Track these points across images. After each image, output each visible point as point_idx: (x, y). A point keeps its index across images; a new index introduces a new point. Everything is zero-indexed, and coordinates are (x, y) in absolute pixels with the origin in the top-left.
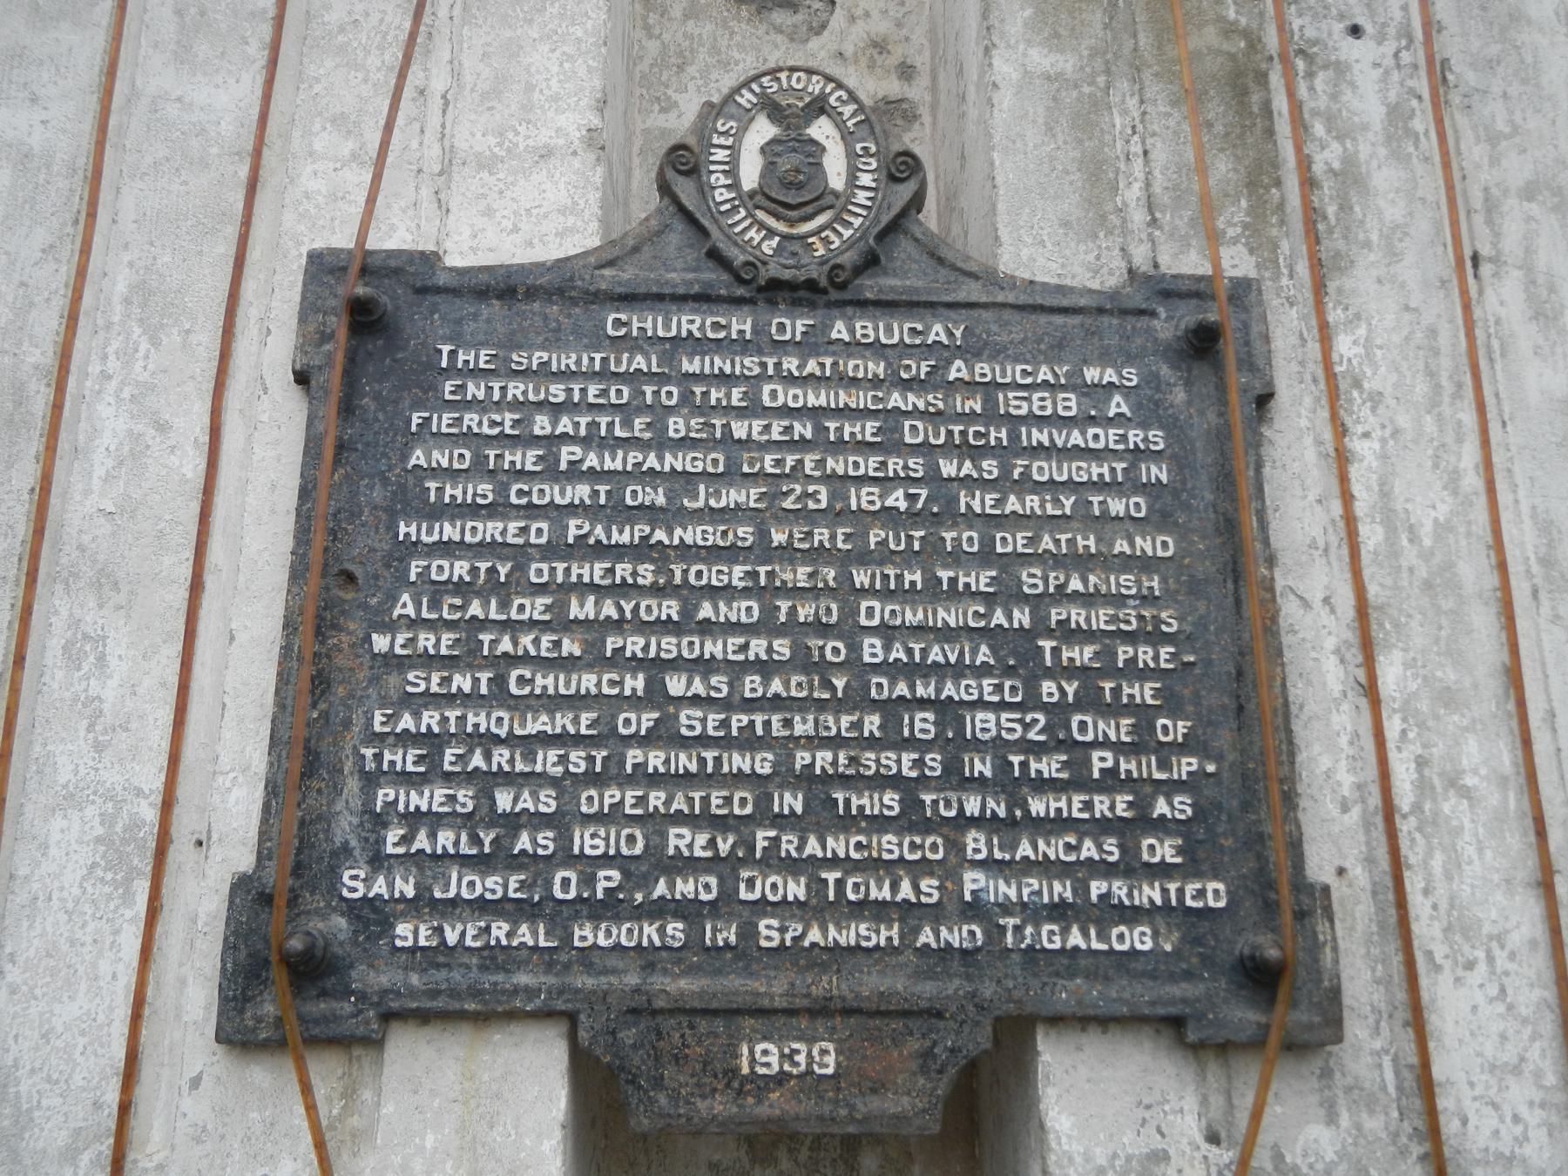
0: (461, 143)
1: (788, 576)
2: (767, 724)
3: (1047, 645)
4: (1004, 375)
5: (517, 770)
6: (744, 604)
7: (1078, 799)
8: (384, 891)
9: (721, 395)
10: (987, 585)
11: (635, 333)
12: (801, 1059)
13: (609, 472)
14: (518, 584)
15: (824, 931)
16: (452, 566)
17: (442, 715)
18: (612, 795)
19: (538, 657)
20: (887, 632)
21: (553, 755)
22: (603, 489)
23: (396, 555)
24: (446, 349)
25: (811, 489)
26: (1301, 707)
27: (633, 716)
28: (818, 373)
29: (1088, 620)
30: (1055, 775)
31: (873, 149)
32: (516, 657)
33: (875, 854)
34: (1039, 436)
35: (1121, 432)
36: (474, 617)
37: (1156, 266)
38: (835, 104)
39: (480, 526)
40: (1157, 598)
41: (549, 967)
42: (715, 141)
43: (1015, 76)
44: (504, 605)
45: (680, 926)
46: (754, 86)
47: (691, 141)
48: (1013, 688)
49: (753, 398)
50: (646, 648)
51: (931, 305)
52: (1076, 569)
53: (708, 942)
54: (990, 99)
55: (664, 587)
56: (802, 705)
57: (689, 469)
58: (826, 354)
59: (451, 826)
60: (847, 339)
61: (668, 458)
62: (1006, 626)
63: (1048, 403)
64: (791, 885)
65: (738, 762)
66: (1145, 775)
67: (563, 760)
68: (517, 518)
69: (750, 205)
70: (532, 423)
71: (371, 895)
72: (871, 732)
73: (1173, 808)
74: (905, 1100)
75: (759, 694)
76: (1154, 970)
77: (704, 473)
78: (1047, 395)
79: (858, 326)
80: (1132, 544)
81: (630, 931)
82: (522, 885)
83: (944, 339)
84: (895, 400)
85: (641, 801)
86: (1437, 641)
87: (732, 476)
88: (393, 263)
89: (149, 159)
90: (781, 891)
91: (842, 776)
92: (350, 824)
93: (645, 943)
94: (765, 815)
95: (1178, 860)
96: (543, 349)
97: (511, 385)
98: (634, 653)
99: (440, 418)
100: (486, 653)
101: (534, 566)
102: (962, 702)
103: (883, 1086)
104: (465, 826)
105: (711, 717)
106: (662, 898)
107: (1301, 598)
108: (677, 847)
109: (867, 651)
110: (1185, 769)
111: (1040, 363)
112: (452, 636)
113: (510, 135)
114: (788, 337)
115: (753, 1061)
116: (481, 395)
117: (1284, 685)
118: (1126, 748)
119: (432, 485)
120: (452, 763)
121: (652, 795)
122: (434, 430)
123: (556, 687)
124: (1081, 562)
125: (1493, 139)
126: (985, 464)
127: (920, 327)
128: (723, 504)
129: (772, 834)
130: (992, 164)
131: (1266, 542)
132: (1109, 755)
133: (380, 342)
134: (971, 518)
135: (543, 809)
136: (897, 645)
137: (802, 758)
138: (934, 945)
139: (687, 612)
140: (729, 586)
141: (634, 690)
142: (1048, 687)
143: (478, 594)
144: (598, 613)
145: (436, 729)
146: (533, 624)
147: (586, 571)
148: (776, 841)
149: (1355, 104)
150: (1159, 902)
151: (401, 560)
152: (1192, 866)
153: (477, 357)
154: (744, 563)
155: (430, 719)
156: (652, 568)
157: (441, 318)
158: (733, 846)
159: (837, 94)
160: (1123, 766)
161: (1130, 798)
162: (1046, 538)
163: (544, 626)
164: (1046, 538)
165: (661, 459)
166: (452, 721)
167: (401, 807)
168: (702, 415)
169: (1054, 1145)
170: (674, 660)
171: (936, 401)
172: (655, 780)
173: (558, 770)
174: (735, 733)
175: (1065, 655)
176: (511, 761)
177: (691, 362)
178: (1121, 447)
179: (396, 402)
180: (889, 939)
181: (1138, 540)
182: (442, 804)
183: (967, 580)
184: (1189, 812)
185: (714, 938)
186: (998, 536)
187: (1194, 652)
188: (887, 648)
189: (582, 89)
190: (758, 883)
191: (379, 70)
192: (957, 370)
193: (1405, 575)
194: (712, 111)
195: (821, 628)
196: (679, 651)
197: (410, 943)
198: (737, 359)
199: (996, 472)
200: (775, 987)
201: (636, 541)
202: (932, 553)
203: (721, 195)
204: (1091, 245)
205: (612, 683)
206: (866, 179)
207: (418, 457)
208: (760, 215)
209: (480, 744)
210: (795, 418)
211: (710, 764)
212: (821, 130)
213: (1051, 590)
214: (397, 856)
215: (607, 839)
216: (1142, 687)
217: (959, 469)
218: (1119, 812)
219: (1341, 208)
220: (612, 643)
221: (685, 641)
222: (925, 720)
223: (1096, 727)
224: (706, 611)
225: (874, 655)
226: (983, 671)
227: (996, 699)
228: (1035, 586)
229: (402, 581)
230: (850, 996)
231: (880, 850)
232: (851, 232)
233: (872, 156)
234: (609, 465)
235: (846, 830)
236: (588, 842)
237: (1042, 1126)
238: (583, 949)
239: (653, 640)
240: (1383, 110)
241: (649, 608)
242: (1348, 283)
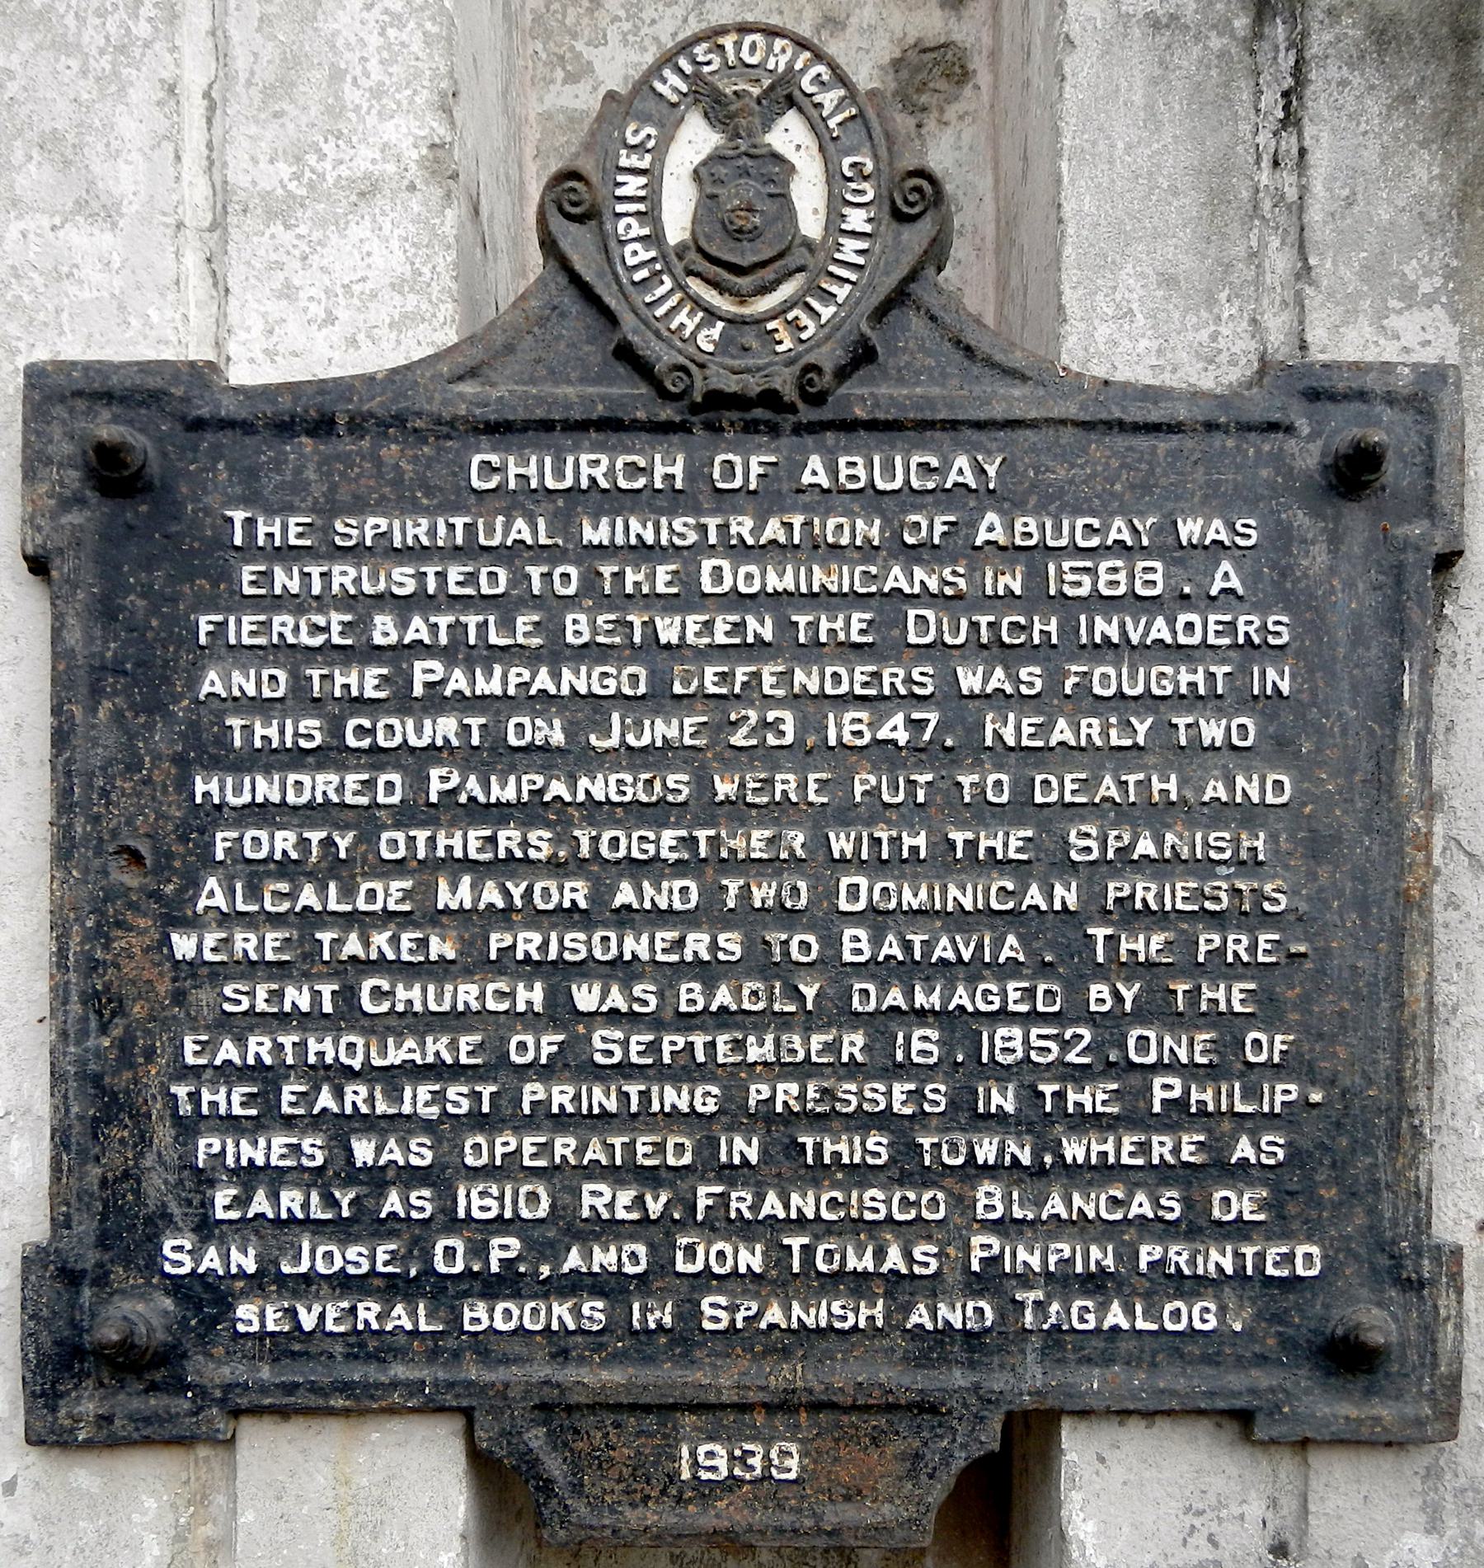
0: (238, 175)
1: (738, 843)
2: (711, 1046)
3: (1100, 932)
5: (378, 1111)
6: (678, 884)
8: (217, 1265)
9: (640, 577)
10: (1019, 850)
11: (512, 485)
12: (756, 1461)
13: (484, 697)
14: (364, 861)
15: (787, 1311)
16: (272, 837)
17: (274, 1041)
18: (505, 1143)
20: (877, 919)
21: (424, 1092)
22: (475, 722)
23: (195, 823)
24: (239, 516)
26: (1454, 1010)
27: (529, 1040)
28: (782, 540)
29: (1160, 896)
30: (1100, 1109)
31: (869, 167)
32: (369, 962)
33: (854, 1213)
34: (1106, 628)
35: (1227, 618)
37: (1303, 346)
38: (809, 89)
39: (306, 779)
40: (1261, 863)
41: (433, 1355)
42: (624, 162)
44: (348, 893)
45: (600, 1305)
46: (683, 63)
47: (587, 166)
49: (687, 579)
50: (544, 947)
51: (953, 425)
52: (1149, 825)
53: (636, 1324)
54: (1059, 66)
55: (566, 862)
56: (758, 1022)
58: (793, 509)
59: (296, 1185)
60: (826, 484)
62: (1044, 907)
63: (1121, 577)
65: (673, 1097)
66: (1224, 1108)
67: (439, 1097)
68: (357, 769)
69: (679, 269)
71: (201, 1270)
72: (852, 1055)
73: (1259, 1150)
74: (886, 1509)
75: (699, 1007)
76: (1218, 1354)
77: (619, 696)
78: (1119, 563)
79: (842, 461)
80: (1231, 786)
81: (535, 1311)
84: (896, 578)
85: (546, 1149)
87: (660, 700)
88: (153, 382)
90: (730, 1262)
92: (166, 1182)
93: (555, 1326)
94: (709, 1166)
95: (1261, 1217)
97: (336, 569)
98: (527, 953)
99: (239, 622)
100: (326, 957)
101: (385, 836)
102: (978, 1013)
103: (859, 1493)
104: (315, 1184)
105: (634, 1039)
108: (592, 1208)
109: (847, 945)
111: (1112, 514)
112: (279, 935)
113: (312, 159)
114: (737, 483)
115: (695, 1464)
116: (294, 586)
118: (1201, 1071)
119: (235, 722)
120: (292, 1104)
121: (559, 1142)
122: (232, 641)
123: (425, 1003)
124: (1155, 814)
126: (1023, 674)
127: (934, 462)
128: (646, 740)
129: (718, 1189)
130: (1059, 181)
131: (1426, 779)
132: (1176, 1082)
133: (143, 508)
134: (1003, 754)
135: (415, 1161)
136: (890, 937)
137: (758, 1092)
138: (929, 1326)
139: (601, 894)
140: (657, 858)
141: (529, 1003)
143: (311, 876)
144: (477, 899)
146: (388, 916)
147: (457, 842)
148: (724, 1198)
150: (1229, 1271)
151: (202, 831)
152: (1280, 1222)
153: (285, 528)
154: (677, 825)
155: (259, 1047)
156: (547, 835)
157: (231, 468)
159: (813, 72)
160: (1195, 1096)
161: (1202, 1138)
162: (1108, 780)
163: (403, 920)
164: (1108, 780)
165: (556, 676)
166: (289, 1049)
167: (230, 1161)
169: (1075, 1555)
170: (583, 962)
172: (562, 1121)
173: (433, 1111)
174: (667, 1060)
175: (1124, 946)
177: (596, 527)
179: (174, 600)
180: (871, 1318)
181: (1240, 781)
182: (282, 1157)
183: (991, 843)
186: (1039, 778)
187: (1308, 939)
188: (877, 942)
189: (418, 75)
190: (700, 1250)
191: (102, 52)
192: (990, 528)
194: (619, 107)
195: (786, 916)
196: (590, 950)
197: (255, 1328)
198: (664, 521)
199: (1039, 683)
200: (724, 1378)
201: (525, 797)
202: (947, 804)
204: (1204, 314)
205: (500, 995)
206: (856, 219)
207: (212, 682)
208: (695, 286)
209: (328, 1079)
210: (747, 611)
211: (634, 1100)
212: (788, 135)
213: (1110, 855)
214: (230, 1222)
216: (1229, 989)
217: (985, 681)
218: (1185, 1157)
220: (497, 941)
222: (925, 1039)
223: (1160, 1044)
224: (625, 895)
225: (859, 952)
226: (1012, 969)
227: (1024, 1008)
228: (1088, 850)
229: (208, 861)
230: (818, 1388)
231: (861, 1208)
232: (833, 309)
233: (866, 178)
234: (482, 687)
235: (816, 1184)
236: (476, 1202)
237: (1062, 1536)
238: (476, 1334)
239: (554, 936)
241: (546, 891)
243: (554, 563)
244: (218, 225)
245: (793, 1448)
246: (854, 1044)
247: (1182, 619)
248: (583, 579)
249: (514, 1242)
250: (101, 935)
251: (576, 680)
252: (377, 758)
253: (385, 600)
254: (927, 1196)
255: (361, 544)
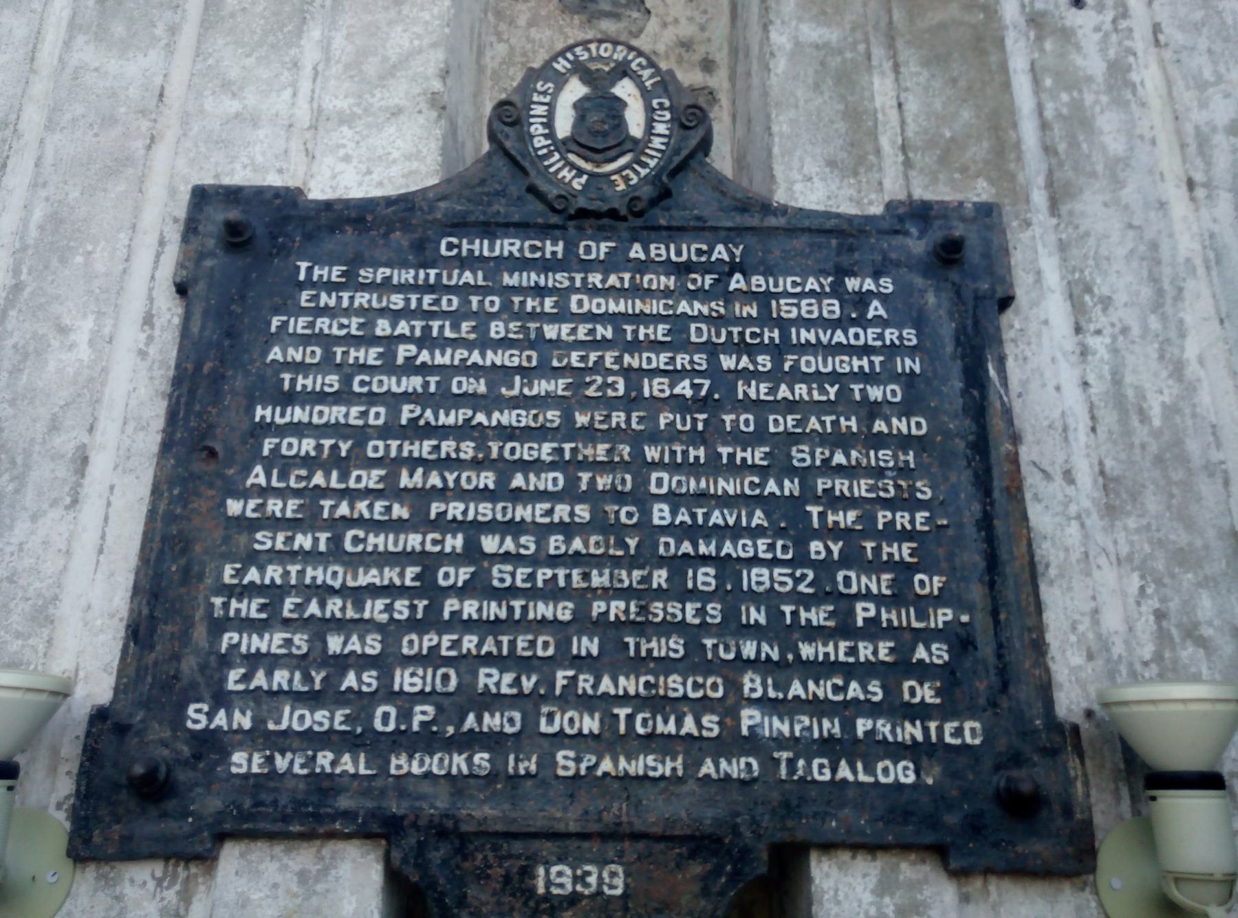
1: (589, 452)
2: (568, 577)
3: (814, 510)
4: (776, 285)
6: (551, 475)
7: (843, 645)
9: (536, 304)
12: (592, 880)
15: (616, 763)
18: (430, 640)
19: (371, 519)
21: (380, 604)
24: (303, 265)
25: (610, 379)
27: (452, 570)
28: (618, 285)
29: (851, 488)
30: (822, 623)
33: (661, 692)
34: (807, 335)
36: (317, 487)
39: (326, 410)
41: (366, 793)
43: (789, 46)
44: (344, 477)
46: (569, 56)
47: (516, 99)
48: (784, 547)
50: (465, 513)
56: (599, 561)
57: (507, 363)
58: (625, 270)
61: (490, 354)
62: (778, 493)
63: (815, 308)
64: (586, 719)
65: (543, 610)
66: (905, 624)
70: (374, 325)
79: (652, 246)
80: (889, 425)
82: (347, 719)
83: (726, 257)
84: (683, 307)
85: (456, 644)
86: (1169, 507)
87: (545, 370)
89: (68, 116)
90: (577, 725)
91: (633, 622)
94: (565, 657)
95: (938, 701)
96: (386, 265)
97: (358, 294)
100: (326, 515)
102: (739, 559)
106: (471, 730)
107: (1043, 471)
110: (941, 619)
114: (593, 256)
115: (549, 883)
117: (1030, 545)
119: (287, 377)
123: (386, 545)
125: (1202, 86)
126: (760, 359)
128: (535, 392)
129: (571, 673)
135: (369, 651)
136: (683, 510)
137: (598, 607)
138: (714, 776)
142: (816, 546)
144: (425, 483)
145: (278, 581)
146: (368, 493)
148: (574, 679)
149: (1079, 61)
155: (273, 573)
158: (536, 684)
160: (884, 616)
162: (813, 419)
164: (813, 419)
165: (483, 356)
166: (293, 575)
167: (243, 649)
168: (518, 320)
171: (718, 307)
172: (469, 625)
173: (384, 618)
174: (540, 584)
175: (831, 518)
176: (343, 609)
178: (879, 343)
180: (674, 769)
181: (895, 421)
184: (946, 657)
185: (516, 768)
186: (771, 418)
187: (946, 516)
188: (674, 513)
193: (1137, 451)
194: (532, 75)
197: (243, 770)
199: (769, 366)
203: (539, 142)
207: (276, 354)
208: (572, 157)
209: (316, 595)
212: (624, 89)
214: (238, 692)
215: (424, 678)
219: (1071, 145)
220: (435, 508)
221: (499, 506)
222: (706, 574)
224: (518, 481)
225: (662, 518)
226: (759, 532)
227: (769, 556)
228: (803, 460)
229: (256, 457)
231: (666, 688)
234: (439, 360)
236: (407, 680)
239: (472, 506)
240: (1104, 65)
242: (1078, 207)
243: (485, 295)
244: (314, 127)
245: (620, 870)
246: (660, 577)
247: (852, 331)
248: (502, 303)
249: (430, 709)
250: (184, 500)
251: (494, 357)
252: (372, 398)
253: (383, 312)
254: (710, 681)
255: (373, 282)
